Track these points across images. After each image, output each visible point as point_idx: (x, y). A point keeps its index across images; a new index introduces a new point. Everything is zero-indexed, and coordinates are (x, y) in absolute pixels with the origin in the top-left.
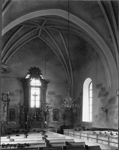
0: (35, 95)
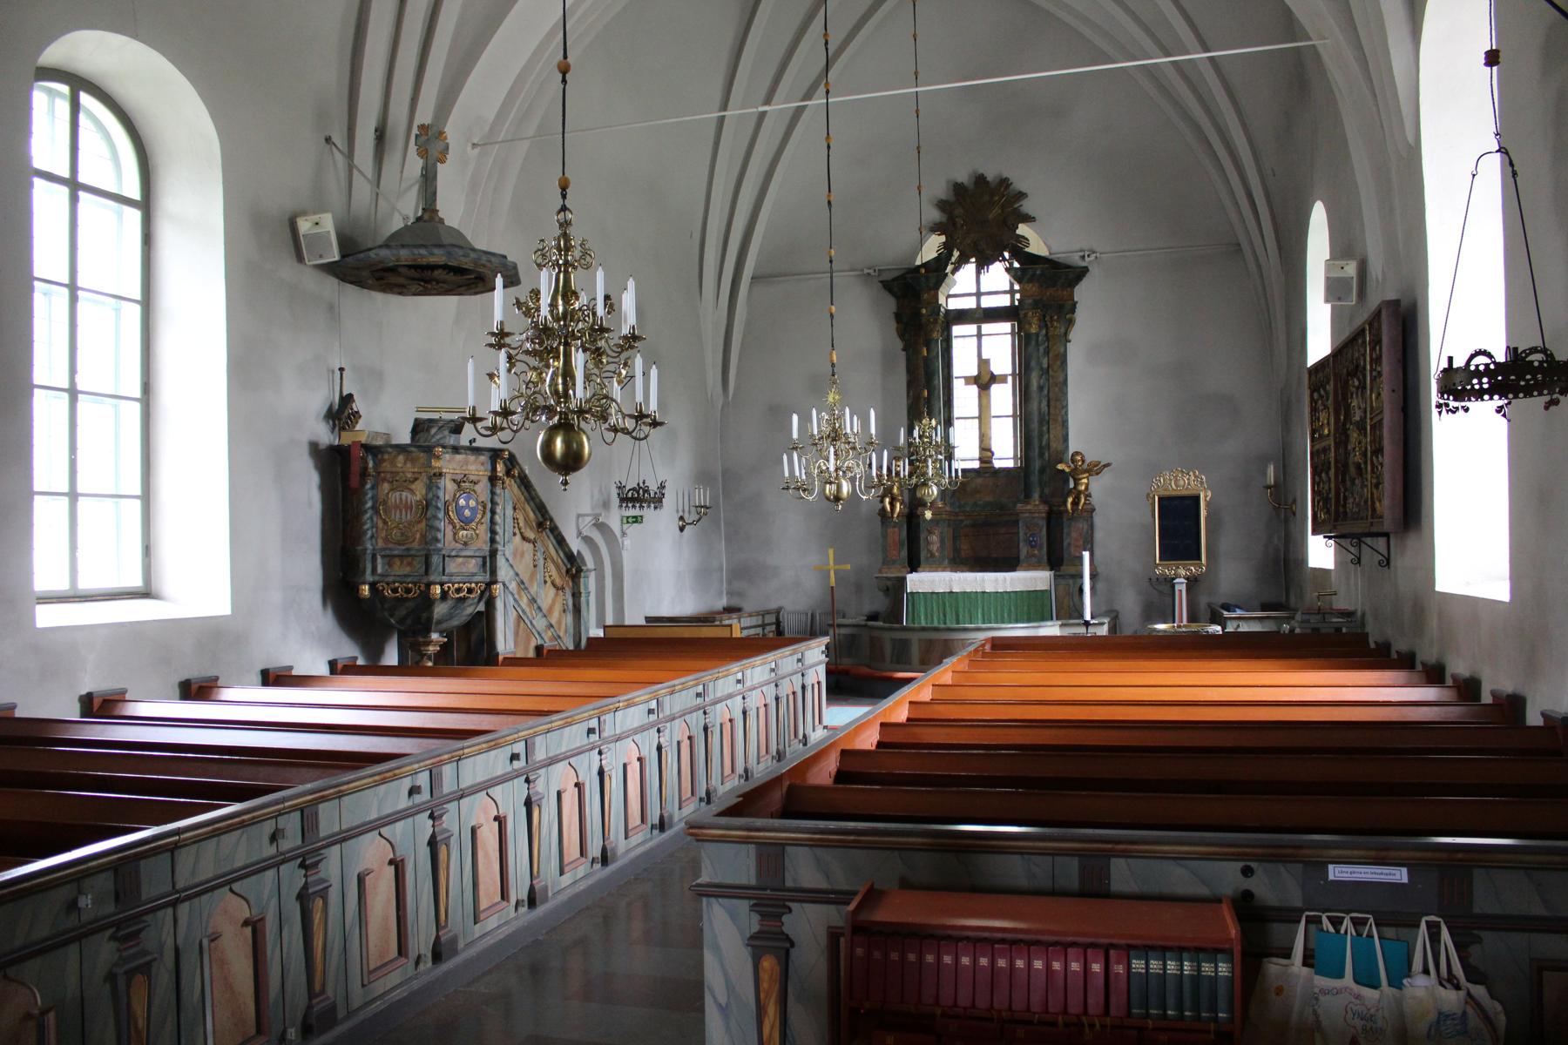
0: (984, 381)
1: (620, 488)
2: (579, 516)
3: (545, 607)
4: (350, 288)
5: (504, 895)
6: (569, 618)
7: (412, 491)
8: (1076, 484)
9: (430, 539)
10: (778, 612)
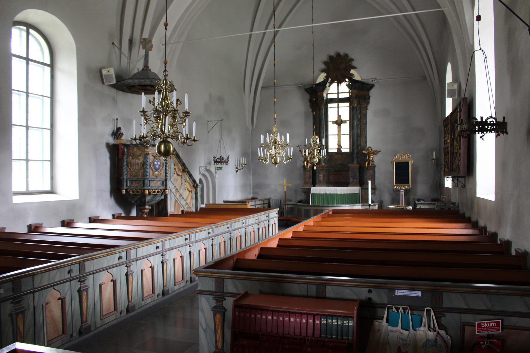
0: (339, 122)
1: (214, 158)
2: (200, 167)
3: (185, 197)
4: (121, 93)
5: (153, 292)
6: (194, 201)
8: (369, 158)
9: (145, 175)
10: (269, 199)
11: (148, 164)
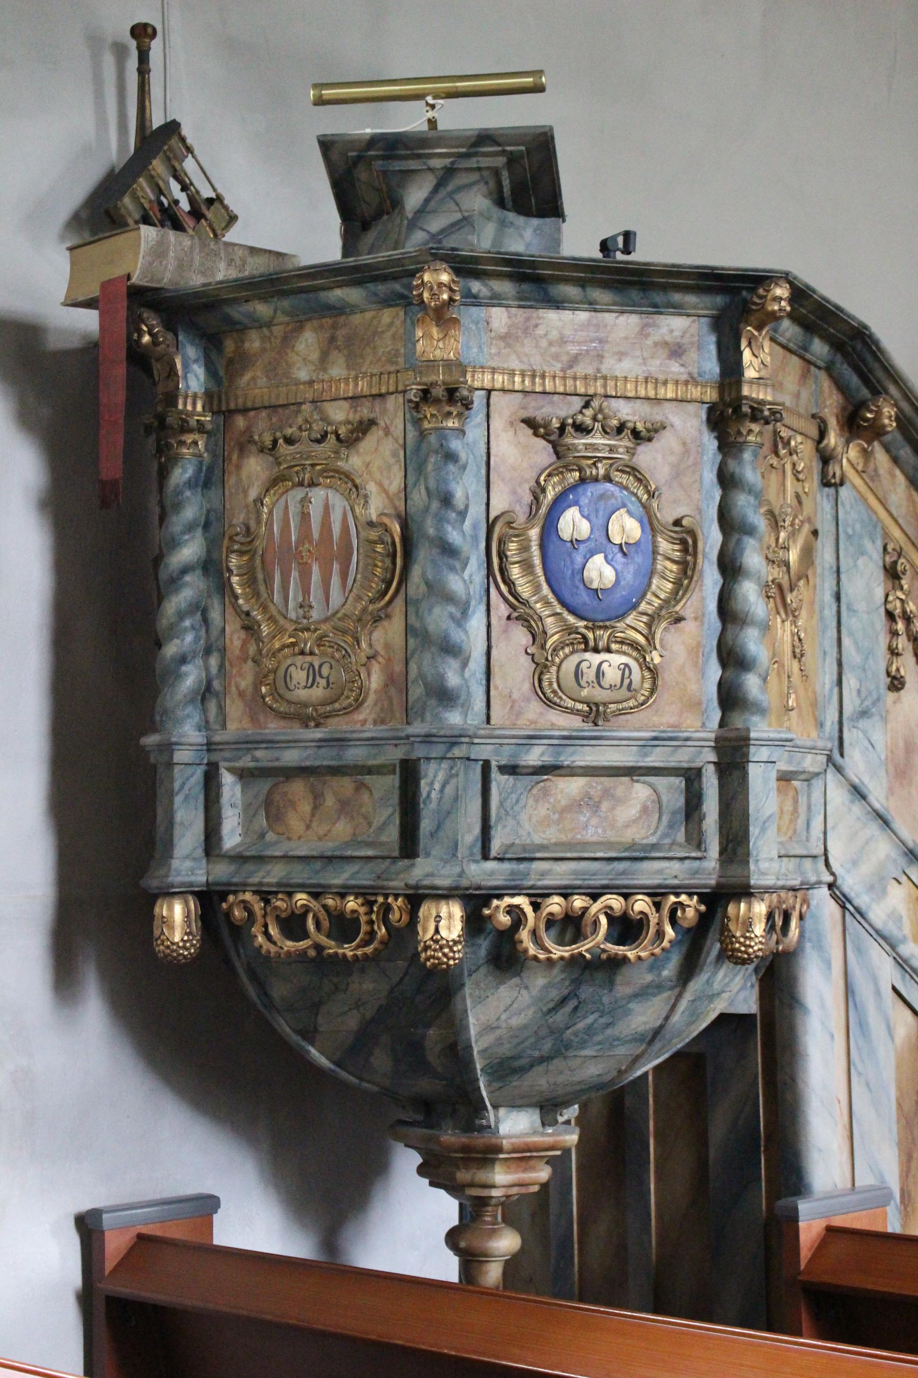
7: (353, 486)
11: (465, 534)
